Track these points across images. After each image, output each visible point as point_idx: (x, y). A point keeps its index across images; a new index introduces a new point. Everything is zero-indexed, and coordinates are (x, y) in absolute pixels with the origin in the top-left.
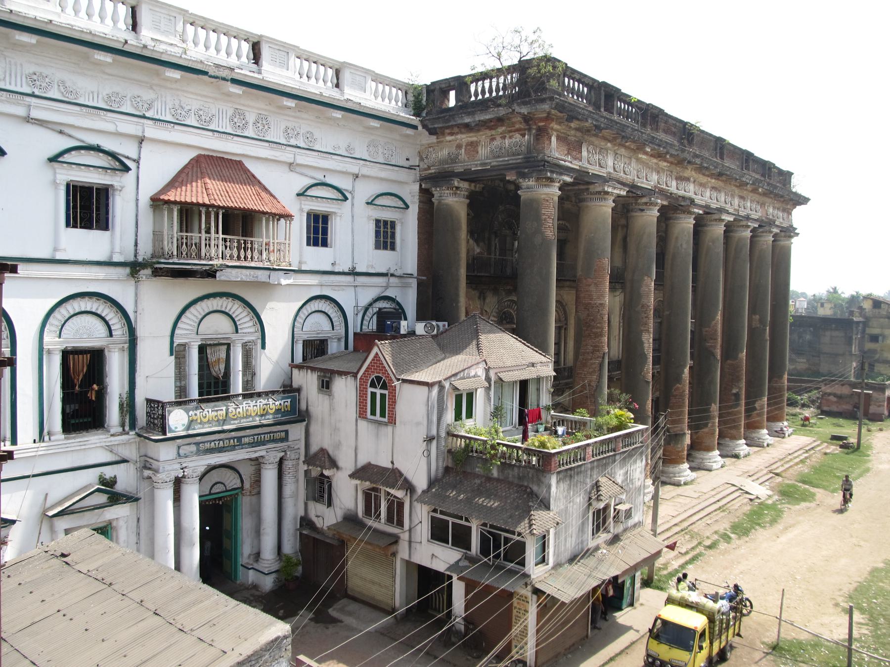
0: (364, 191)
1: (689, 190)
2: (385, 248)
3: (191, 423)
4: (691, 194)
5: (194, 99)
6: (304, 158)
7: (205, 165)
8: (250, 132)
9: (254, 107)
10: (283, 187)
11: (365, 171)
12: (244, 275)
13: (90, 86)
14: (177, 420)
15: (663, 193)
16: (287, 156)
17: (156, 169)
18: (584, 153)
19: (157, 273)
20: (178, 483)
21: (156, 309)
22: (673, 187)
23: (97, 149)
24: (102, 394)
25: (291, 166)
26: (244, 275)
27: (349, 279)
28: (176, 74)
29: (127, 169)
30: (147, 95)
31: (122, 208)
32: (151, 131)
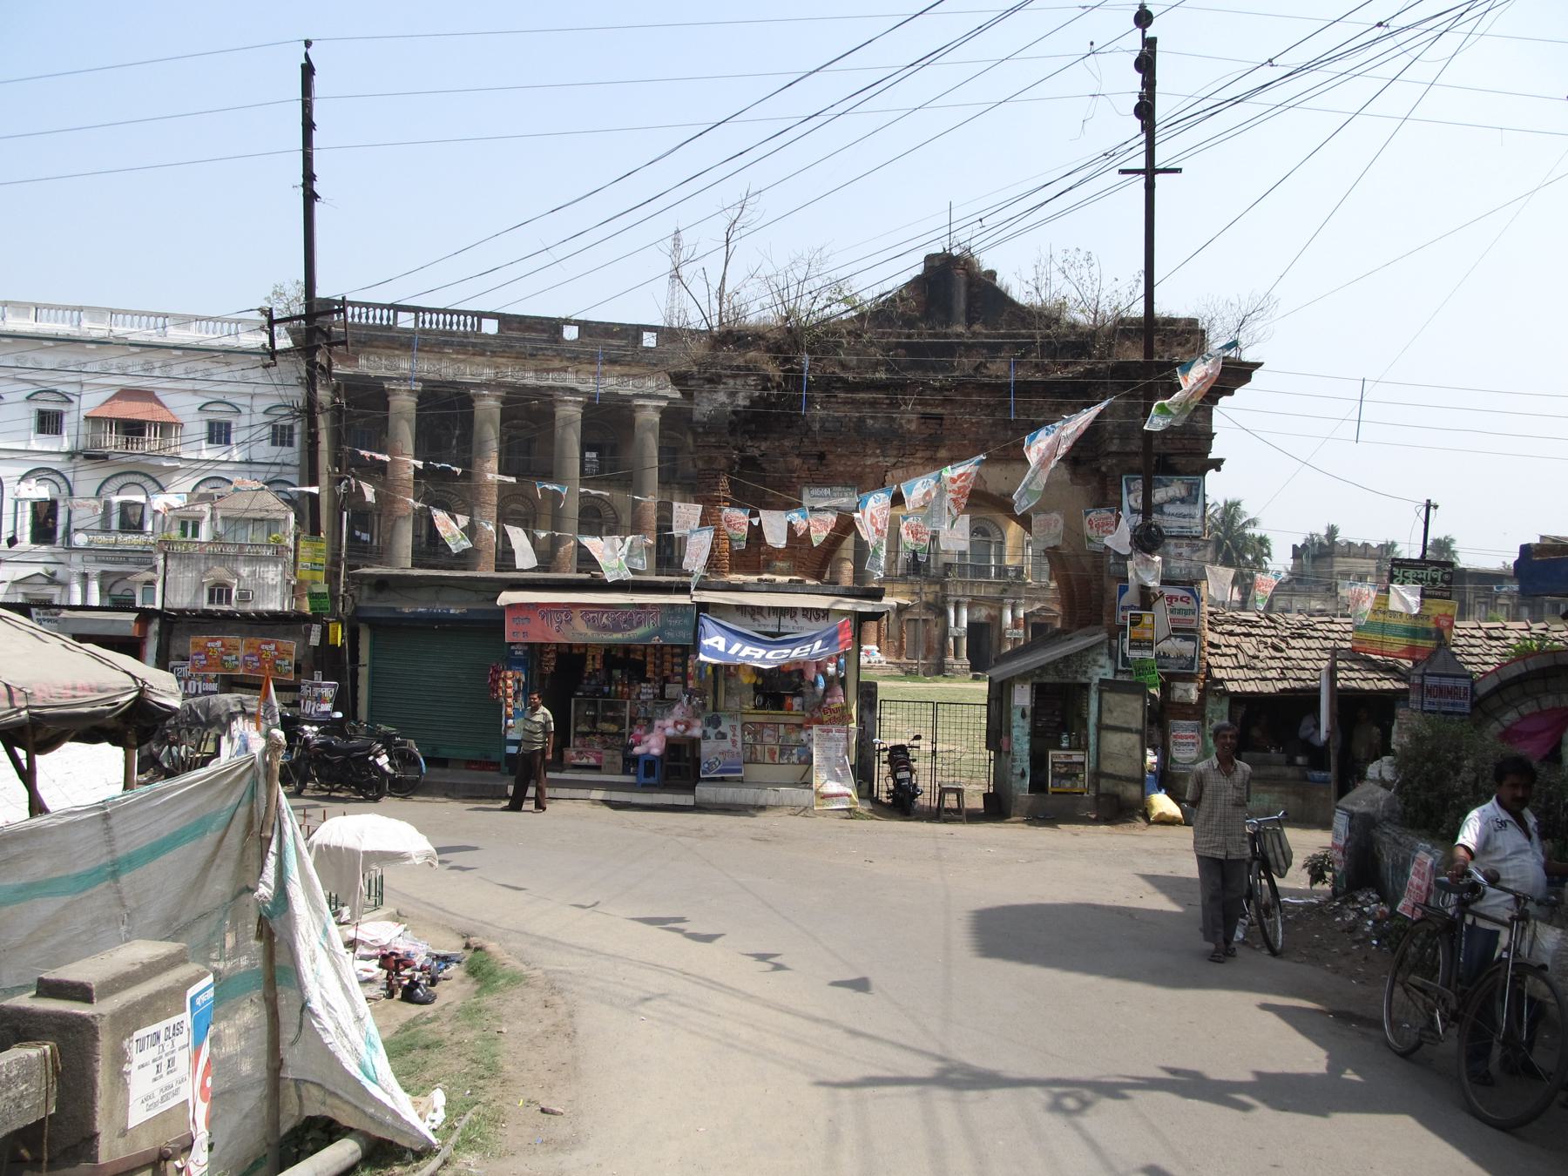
0: (261, 404)
1: (570, 380)
2: (282, 444)
3: (90, 542)
4: (574, 385)
5: (114, 359)
6: (199, 386)
7: (126, 394)
8: (157, 373)
9: (157, 358)
10: (183, 406)
11: (258, 391)
12: (130, 459)
13: (49, 359)
14: (80, 539)
15: (500, 385)
16: (188, 385)
17: (91, 401)
18: (362, 361)
19: (88, 457)
20: (85, 576)
21: (87, 480)
22: (530, 379)
23: (54, 391)
24: (55, 524)
25: (195, 392)
26: (130, 459)
27: (244, 467)
28: (93, 346)
29: (70, 401)
30: (83, 359)
31: (69, 422)
32: (84, 378)
